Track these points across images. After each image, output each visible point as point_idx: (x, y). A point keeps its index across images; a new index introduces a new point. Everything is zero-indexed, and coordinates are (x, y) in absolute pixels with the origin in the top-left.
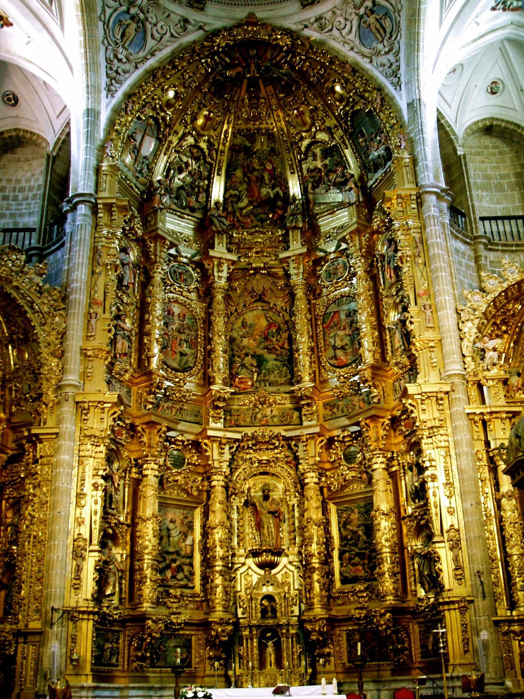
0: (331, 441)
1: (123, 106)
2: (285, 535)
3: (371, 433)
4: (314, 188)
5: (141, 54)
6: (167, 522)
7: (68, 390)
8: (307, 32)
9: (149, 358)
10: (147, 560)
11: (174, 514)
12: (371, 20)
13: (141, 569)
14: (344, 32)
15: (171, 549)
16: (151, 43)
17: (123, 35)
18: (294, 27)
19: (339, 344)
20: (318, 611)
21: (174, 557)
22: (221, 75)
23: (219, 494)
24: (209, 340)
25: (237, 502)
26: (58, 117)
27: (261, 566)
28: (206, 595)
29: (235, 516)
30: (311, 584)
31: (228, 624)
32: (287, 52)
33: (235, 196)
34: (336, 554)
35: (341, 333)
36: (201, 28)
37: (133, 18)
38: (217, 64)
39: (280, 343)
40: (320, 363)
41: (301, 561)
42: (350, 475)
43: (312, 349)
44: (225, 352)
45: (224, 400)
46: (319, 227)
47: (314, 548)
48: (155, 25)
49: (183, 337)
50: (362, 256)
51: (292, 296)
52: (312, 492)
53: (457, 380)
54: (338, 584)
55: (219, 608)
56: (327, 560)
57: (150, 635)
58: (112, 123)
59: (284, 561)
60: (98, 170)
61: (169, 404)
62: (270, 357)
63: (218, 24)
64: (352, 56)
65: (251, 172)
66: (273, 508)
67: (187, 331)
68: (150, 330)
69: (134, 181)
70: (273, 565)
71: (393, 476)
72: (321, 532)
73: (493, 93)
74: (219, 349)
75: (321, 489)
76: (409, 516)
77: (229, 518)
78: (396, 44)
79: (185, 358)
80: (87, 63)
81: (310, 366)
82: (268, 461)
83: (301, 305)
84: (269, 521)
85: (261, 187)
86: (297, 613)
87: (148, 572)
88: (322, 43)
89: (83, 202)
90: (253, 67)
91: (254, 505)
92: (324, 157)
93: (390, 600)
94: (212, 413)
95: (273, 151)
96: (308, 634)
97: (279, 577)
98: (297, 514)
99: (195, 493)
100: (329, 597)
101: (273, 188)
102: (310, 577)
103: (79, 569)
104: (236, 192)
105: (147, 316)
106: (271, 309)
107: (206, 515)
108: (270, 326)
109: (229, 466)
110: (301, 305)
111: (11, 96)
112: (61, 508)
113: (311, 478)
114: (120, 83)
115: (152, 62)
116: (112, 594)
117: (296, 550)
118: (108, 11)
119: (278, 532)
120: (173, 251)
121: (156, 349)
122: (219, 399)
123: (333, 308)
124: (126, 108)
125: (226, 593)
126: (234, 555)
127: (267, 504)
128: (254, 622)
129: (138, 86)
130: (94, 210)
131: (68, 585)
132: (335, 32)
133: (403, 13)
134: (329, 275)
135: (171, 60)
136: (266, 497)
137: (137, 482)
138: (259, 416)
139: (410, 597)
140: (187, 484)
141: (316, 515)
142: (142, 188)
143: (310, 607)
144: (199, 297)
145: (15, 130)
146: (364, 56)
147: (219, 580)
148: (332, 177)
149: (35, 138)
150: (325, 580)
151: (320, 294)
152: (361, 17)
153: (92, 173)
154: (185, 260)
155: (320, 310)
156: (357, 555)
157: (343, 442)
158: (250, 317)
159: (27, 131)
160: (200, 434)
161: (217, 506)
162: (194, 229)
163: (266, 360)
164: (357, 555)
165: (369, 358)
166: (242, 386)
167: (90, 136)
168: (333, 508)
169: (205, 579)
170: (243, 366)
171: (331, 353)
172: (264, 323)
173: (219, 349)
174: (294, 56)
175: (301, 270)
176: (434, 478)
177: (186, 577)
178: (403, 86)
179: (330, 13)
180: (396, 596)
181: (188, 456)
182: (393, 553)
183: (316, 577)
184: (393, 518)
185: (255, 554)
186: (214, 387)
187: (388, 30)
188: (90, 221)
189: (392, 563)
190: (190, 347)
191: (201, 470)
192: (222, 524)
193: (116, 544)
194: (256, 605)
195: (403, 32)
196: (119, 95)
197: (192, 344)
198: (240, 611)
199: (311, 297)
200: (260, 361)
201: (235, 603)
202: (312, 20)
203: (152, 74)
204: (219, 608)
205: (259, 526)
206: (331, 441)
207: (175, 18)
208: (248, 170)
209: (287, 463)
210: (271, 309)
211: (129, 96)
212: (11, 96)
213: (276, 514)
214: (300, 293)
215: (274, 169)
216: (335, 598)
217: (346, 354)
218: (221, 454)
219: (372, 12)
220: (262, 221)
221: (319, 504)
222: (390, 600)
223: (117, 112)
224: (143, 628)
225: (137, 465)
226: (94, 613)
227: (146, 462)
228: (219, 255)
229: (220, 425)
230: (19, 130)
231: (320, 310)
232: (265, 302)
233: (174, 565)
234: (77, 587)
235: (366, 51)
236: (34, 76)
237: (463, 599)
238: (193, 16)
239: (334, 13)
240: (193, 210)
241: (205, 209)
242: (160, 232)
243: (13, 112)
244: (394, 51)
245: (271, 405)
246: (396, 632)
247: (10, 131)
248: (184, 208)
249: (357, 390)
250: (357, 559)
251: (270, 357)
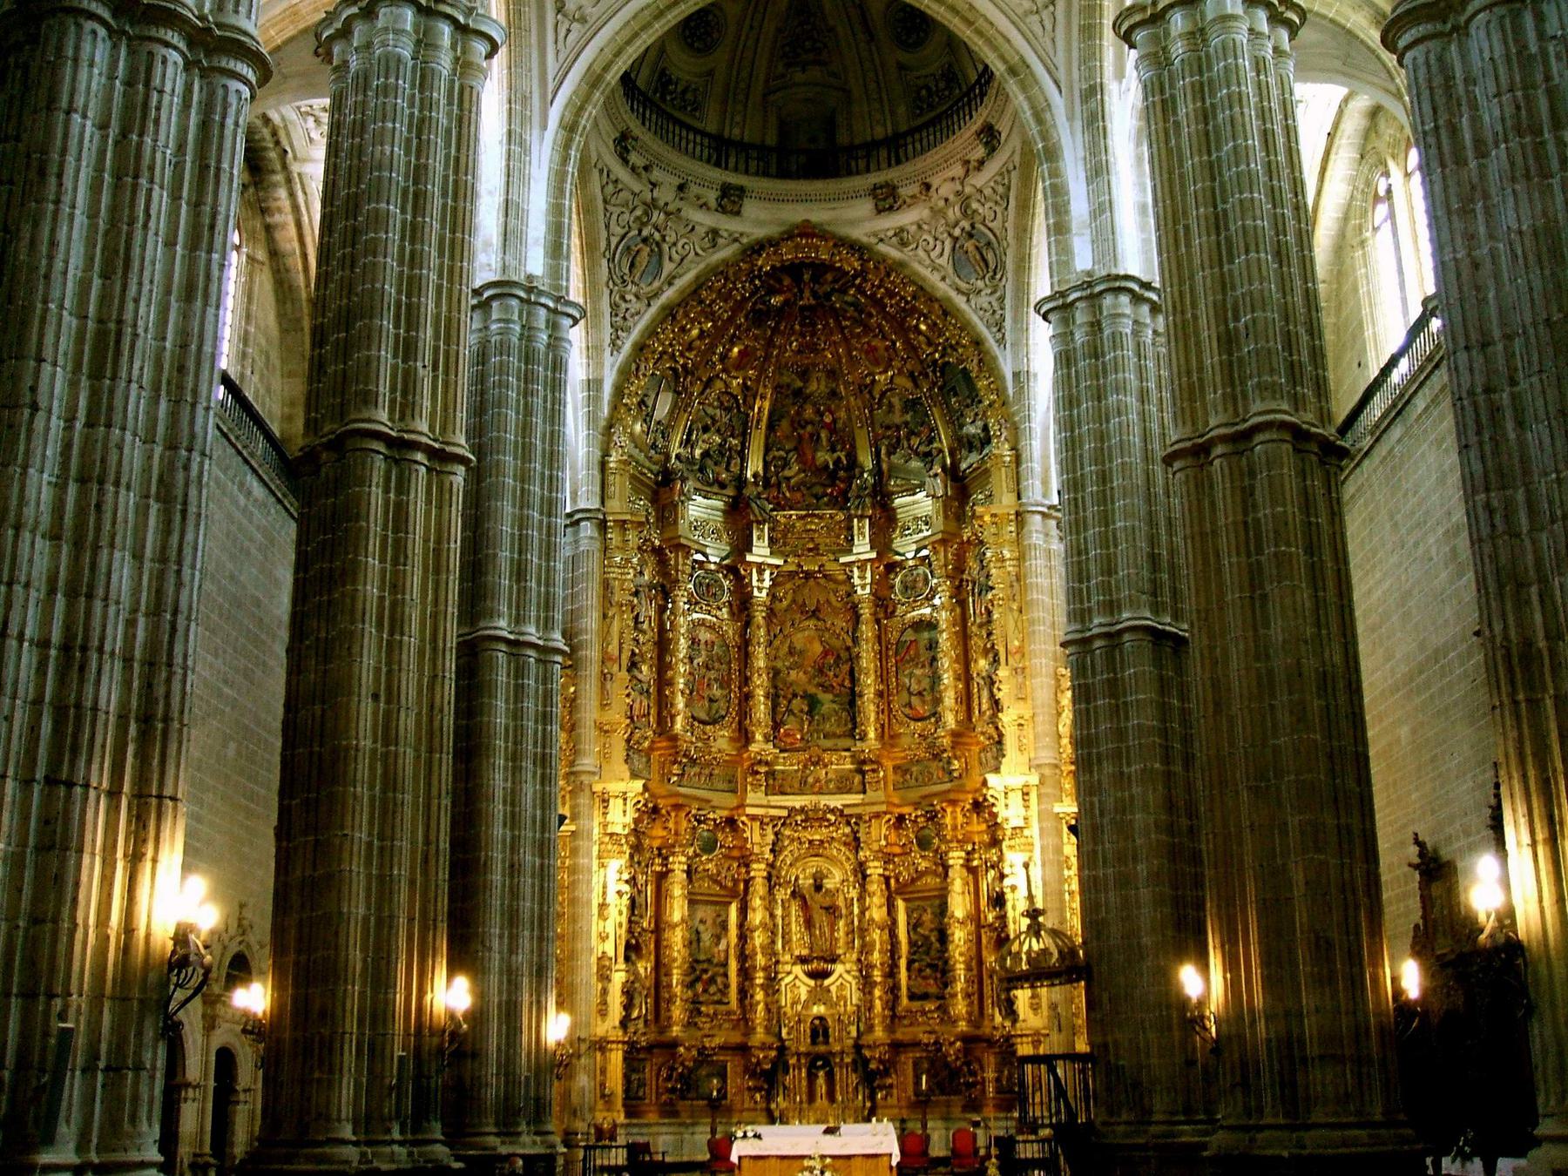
0: (901, 819)
1: (634, 367)
2: (841, 934)
3: (948, 820)
4: (889, 454)
5: (656, 284)
6: (697, 923)
7: (583, 778)
8: (882, 248)
9: (673, 717)
10: (676, 976)
11: (706, 912)
12: (969, 245)
13: (670, 986)
14: (934, 255)
15: (702, 957)
16: (668, 267)
17: (632, 265)
18: (865, 239)
19: (915, 688)
20: (879, 1033)
21: (705, 966)
22: (764, 303)
23: (759, 887)
24: (746, 680)
25: (782, 894)
27: (811, 975)
28: (744, 1012)
29: (779, 912)
30: (871, 1001)
31: (770, 1048)
32: (855, 277)
33: (781, 458)
34: (903, 963)
35: (918, 672)
36: (736, 240)
37: (645, 240)
38: (757, 289)
39: (839, 680)
40: (890, 710)
41: (860, 971)
42: (923, 865)
43: (880, 694)
44: (767, 696)
45: (767, 763)
46: (894, 510)
47: (876, 957)
48: (675, 244)
49: (712, 675)
50: (948, 577)
51: (856, 618)
52: (875, 887)
53: (1047, 771)
54: (905, 1001)
55: (760, 1030)
56: (891, 972)
57: (682, 1064)
58: (619, 392)
59: (839, 968)
60: (603, 466)
61: (697, 769)
62: (825, 698)
63: (760, 233)
64: (943, 288)
65: (803, 428)
66: (827, 902)
67: (717, 665)
68: (673, 678)
69: (647, 464)
70: (826, 974)
71: (972, 871)
72: (886, 937)
74: (760, 692)
75: (887, 879)
76: (990, 925)
77: (772, 916)
79: (715, 705)
81: (877, 719)
82: (822, 842)
83: (867, 631)
84: (820, 918)
85: (816, 451)
86: (854, 1034)
87: (678, 990)
88: (902, 264)
89: (587, 519)
90: (807, 293)
91: (803, 898)
92: (905, 410)
93: (963, 1026)
94: (749, 779)
95: (834, 394)
96: (866, 1061)
97: (833, 989)
98: (856, 911)
99: (730, 884)
100: (894, 1017)
101: (833, 450)
102: (871, 993)
103: (605, 992)
104: (782, 453)
105: (668, 659)
106: (828, 630)
107: (743, 911)
108: (826, 653)
109: (772, 851)
110: (867, 631)
112: (582, 923)
113: (875, 869)
114: (628, 330)
115: (669, 294)
116: (638, 1018)
117: (855, 956)
118: (614, 241)
119: (832, 931)
120: (699, 557)
121: (680, 703)
122: (760, 762)
123: (909, 636)
124: (638, 369)
125: (768, 1010)
126: (777, 962)
127: (818, 897)
128: (802, 1049)
129: (651, 332)
130: (603, 526)
131: (594, 1008)
132: (921, 252)
134: (906, 587)
135: (694, 293)
136: (818, 887)
137: (662, 877)
138: (810, 780)
139: (986, 1022)
140: (719, 873)
141: (878, 913)
142: (655, 468)
143: (871, 1028)
144: (731, 613)
146: (958, 290)
147: (759, 996)
148: (915, 441)
150: (890, 996)
151: (894, 612)
152: (956, 239)
153: (596, 473)
154: (713, 567)
155: (894, 636)
156: (929, 966)
157: (915, 822)
158: (799, 640)
160: (738, 807)
161: (757, 902)
162: (724, 512)
163: (818, 702)
164: (929, 966)
165: (950, 720)
166: (789, 740)
167: (591, 418)
168: (901, 905)
169: (743, 993)
170: (790, 711)
171: (905, 694)
172: (817, 648)
173: (760, 692)
174: (865, 280)
175: (868, 580)
176: (1013, 888)
177: (720, 990)
179: (914, 228)
180: (969, 1021)
181: (720, 836)
182: (969, 969)
183: (877, 992)
184: (971, 927)
185: (803, 960)
186: (754, 748)
187: (992, 266)
188: (598, 545)
189: (967, 981)
190: (721, 687)
191: (736, 853)
192: (764, 925)
193: (640, 956)
194: (805, 1028)
195: (1010, 275)
196: (627, 347)
197: (725, 684)
198: (784, 1031)
199: (881, 615)
200: (813, 703)
201: (779, 1021)
202: (890, 233)
203: (669, 313)
204: (760, 1030)
205: (809, 923)
206: (901, 819)
207: (701, 231)
208: (797, 423)
209: (845, 844)
210: (828, 630)
211: (640, 348)
213: (832, 910)
214: (866, 612)
215: (835, 421)
216: (901, 1018)
217: (924, 702)
218: (763, 836)
219: (971, 236)
220: (818, 498)
221: (884, 900)
222: (963, 1026)
223: (626, 375)
224: (674, 1056)
225: (660, 855)
226: (624, 1043)
227: (673, 854)
228: (760, 560)
229: (761, 795)
231: (894, 636)
232: (819, 619)
233: (705, 977)
234: (603, 1012)
235: (963, 286)
237: (1037, 1033)
238: (727, 224)
239: (920, 227)
240: (723, 486)
241: (740, 481)
242: (683, 541)
245: (826, 766)
246: (968, 1064)
248: (710, 485)
249: (937, 757)
250: (928, 971)
251: (825, 698)
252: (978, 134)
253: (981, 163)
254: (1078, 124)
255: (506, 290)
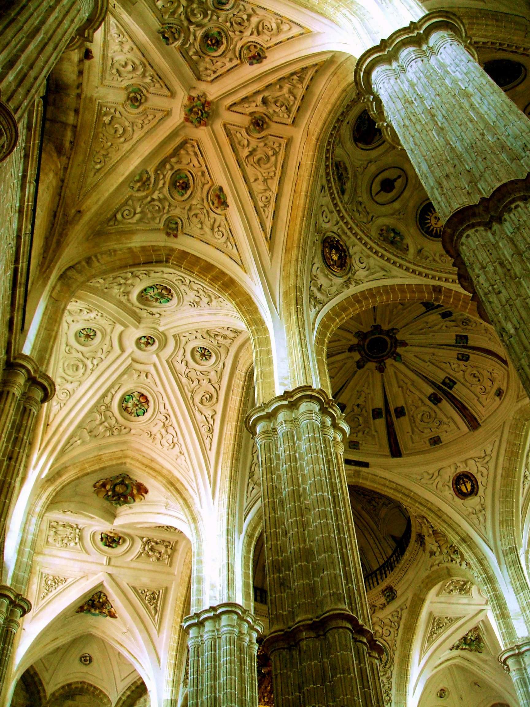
26: (122, 680)
73: (441, 697)
78: (389, 672)
80: (175, 664)
111: (88, 658)
133: (397, 653)
145: (81, 682)
149: (97, 692)
159: (91, 685)
178: (393, 704)
195: (396, 665)
212: (88, 658)
230: (84, 683)
236: (112, 647)
243: (85, 669)
244: (387, 676)
247: (77, 682)
252: (383, 592)
253: (384, 606)
254: (504, 567)
255: (233, 609)
